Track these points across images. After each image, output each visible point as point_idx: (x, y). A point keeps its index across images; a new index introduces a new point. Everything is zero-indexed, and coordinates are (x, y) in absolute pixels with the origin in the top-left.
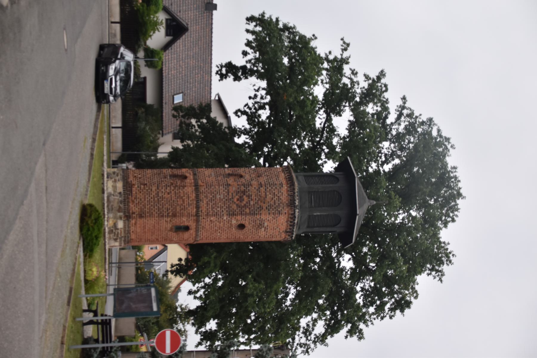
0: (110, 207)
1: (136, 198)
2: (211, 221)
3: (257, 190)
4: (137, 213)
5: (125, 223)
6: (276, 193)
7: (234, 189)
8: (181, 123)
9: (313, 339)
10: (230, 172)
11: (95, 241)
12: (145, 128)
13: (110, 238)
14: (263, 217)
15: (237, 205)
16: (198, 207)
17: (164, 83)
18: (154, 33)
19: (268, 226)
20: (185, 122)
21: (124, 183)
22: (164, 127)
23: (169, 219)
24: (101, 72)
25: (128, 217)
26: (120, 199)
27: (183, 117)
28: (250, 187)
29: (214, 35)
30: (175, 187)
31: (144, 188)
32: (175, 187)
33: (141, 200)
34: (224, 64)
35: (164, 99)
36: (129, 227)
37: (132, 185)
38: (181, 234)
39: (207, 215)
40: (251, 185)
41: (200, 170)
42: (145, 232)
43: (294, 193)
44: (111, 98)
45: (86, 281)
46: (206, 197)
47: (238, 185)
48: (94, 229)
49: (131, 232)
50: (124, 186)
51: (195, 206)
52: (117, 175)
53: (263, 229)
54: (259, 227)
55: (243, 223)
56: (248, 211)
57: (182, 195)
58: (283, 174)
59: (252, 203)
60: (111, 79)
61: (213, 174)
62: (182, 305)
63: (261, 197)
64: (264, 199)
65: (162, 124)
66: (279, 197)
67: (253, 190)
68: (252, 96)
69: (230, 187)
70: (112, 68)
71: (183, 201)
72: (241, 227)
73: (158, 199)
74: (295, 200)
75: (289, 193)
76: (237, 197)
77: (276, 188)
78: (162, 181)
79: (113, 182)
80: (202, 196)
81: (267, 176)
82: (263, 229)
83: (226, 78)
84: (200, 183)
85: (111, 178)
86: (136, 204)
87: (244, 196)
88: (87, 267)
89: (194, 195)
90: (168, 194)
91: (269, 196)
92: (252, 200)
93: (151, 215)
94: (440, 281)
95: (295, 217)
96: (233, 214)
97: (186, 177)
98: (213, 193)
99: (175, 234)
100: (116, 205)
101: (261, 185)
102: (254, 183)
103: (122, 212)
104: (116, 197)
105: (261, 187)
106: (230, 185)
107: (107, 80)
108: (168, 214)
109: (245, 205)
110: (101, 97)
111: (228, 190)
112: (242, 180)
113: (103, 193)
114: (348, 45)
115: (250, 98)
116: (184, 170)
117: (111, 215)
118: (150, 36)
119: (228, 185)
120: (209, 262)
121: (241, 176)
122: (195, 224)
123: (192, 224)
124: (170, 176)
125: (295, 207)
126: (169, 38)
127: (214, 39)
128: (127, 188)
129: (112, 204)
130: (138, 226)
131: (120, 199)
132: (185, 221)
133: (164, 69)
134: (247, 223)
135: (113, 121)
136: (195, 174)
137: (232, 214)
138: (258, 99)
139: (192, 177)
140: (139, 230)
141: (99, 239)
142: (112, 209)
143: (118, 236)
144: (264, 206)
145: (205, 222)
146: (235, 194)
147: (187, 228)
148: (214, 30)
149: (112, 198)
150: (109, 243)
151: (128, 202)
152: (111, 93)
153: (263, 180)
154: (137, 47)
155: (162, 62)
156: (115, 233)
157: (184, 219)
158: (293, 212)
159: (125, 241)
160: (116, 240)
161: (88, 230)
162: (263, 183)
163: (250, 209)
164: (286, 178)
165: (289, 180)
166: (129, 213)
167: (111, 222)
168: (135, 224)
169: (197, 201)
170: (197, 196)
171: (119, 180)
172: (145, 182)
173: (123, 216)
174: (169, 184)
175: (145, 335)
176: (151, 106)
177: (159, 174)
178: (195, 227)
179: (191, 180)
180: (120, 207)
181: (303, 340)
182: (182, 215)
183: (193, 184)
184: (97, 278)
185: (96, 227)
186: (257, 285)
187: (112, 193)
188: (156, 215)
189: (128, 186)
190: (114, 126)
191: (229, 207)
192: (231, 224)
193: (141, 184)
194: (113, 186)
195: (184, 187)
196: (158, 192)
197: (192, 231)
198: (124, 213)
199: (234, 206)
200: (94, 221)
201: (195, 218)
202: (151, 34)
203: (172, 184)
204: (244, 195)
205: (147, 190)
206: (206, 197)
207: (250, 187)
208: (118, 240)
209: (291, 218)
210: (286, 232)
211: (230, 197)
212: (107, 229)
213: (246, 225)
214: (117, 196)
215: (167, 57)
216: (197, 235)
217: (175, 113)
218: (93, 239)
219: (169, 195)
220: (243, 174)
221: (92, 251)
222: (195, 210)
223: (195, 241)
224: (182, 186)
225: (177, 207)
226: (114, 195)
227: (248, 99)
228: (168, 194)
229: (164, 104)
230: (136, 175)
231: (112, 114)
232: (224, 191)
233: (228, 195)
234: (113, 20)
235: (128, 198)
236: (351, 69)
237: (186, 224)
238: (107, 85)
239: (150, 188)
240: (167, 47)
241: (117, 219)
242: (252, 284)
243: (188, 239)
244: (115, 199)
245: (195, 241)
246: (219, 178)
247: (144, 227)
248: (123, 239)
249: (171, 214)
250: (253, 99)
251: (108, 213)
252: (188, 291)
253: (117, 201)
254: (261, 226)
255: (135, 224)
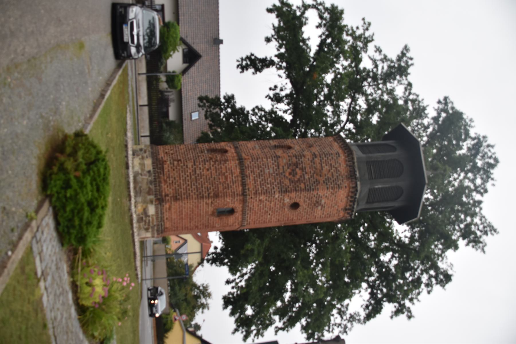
0: (138, 189)
1: (168, 177)
2: (260, 200)
3: (311, 161)
4: (172, 195)
5: (157, 208)
6: (333, 164)
7: (285, 161)
8: (206, 111)
9: (348, 318)
10: (277, 144)
11: (86, 214)
12: (169, 137)
13: (139, 228)
14: (321, 193)
15: (290, 180)
16: (244, 185)
17: (183, 102)
18: (174, 52)
19: (325, 203)
20: (210, 111)
21: (153, 160)
22: (185, 139)
23: (210, 201)
24: (118, 14)
25: (160, 200)
26: (150, 178)
27: (210, 107)
28: (303, 158)
29: (221, 65)
30: (215, 162)
31: (178, 165)
32: (215, 162)
33: (175, 178)
34: (244, 58)
35: (184, 115)
36: (162, 213)
37: (163, 163)
38: (224, 218)
39: (256, 193)
40: (304, 156)
41: (241, 143)
42: (182, 218)
43: (354, 163)
44: (133, 50)
45: (81, 310)
46: (253, 172)
47: (289, 156)
48: (82, 186)
49: (165, 218)
50: (153, 163)
51: (240, 183)
52: (145, 152)
53: (320, 208)
54: (315, 204)
55: (298, 201)
56: (302, 186)
57: (224, 171)
58: (336, 144)
59: (306, 177)
60: (132, 24)
61: (257, 146)
62: (203, 284)
63: (316, 169)
64: (320, 171)
65: (183, 136)
66: (336, 168)
67: (306, 161)
68: (273, 87)
69: (280, 159)
70: (132, 11)
71: (226, 178)
72: (295, 206)
73: (196, 177)
74: (355, 171)
75: (348, 163)
76: (289, 170)
77: (332, 158)
78: (198, 156)
79: (140, 159)
80: (248, 172)
81: (320, 146)
82: (320, 208)
83: (247, 70)
84: (244, 156)
85: (138, 155)
86: (170, 184)
87: (297, 170)
88: (79, 277)
89: (238, 170)
90: (208, 170)
91: (326, 168)
92: (306, 173)
93: (188, 197)
94: (482, 253)
95: (357, 190)
96: (286, 191)
97: (226, 151)
98: (261, 167)
99: (217, 219)
100: (145, 186)
101: (314, 155)
102: (306, 153)
103: (152, 194)
104: (144, 177)
105: (316, 157)
106: (279, 157)
107: (127, 24)
108: (209, 194)
109: (299, 180)
110: (120, 49)
111: (278, 163)
112: (292, 151)
113: (127, 168)
114: (369, 24)
115: (270, 89)
116: (223, 144)
117: (139, 199)
118: (171, 56)
119: (278, 157)
120: (252, 251)
121: (289, 148)
122: (241, 205)
123: (238, 206)
124: (208, 150)
125: (356, 178)
126: (186, 65)
127: (221, 69)
128: (157, 165)
129: (140, 185)
130: (174, 211)
131: (150, 178)
132: (229, 202)
133: (183, 90)
134: (302, 200)
135: (142, 131)
136: (236, 148)
137: (285, 191)
138: (278, 91)
139: (233, 150)
140: (174, 216)
141: (99, 211)
142: (141, 191)
143: (149, 225)
144: (321, 180)
145: (253, 203)
146: (286, 168)
147: (232, 212)
148: (221, 61)
149: (139, 178)
150: (138, 235)
151: (160, 182)
152: (133, 42)
153: (316, 150)
154: (159, 64)
155: (181, 85)
156: (145, 221)
157: (229, 200)
158: (354, 185)
159: (158, 230)
160: (147, 230)
161: (67, 185)
162: (317, 153)
163: (305, 183)
164: (340, 147)
165: (346, 149)
166: (161, 195)
167: (140, 208)
168: (170, 208)
169: (242, 177)
170: (242, 172)
171: (147, 157)
172: (179, 158)
173: (154, 199)
174: (208, 159)
175: (177, 310)
176: (173, 122)
177: (194, 149)
178: (241, 209)
179: (232, 153)
180: (150, 189)
181: (338, 320)
182: (225, 195)
183: (236, 158)
184: (106, 299)
185: (87, 180)
186: (306, 271)
187: (140, 171)
188: (194, 196)
189: (158, 164)
190: (142, 135)
191: (281, 183)
192: (284, 204)
193: (174, 160)
194: (140, 164)
195: (226, 161)
196: (195, 169)
197: (238, 215)
198: (156, 195)
199: (287, 182)
200: (84, 167)
201: (241, 198)
202: (172, 53)
203: (211, 159)
204: (297, 167)
205: (182, 167)
206: (253, 172)
207: (303, 158)
208: (150, 230)
209: (352, 192)
210: (345, 209)
211: (281, 171)
212: (134, 216)
213: (300, 204)
214: (145, 175)
215: (185, 81)
216: (243, 219)
217: (201, 104)
218: (81, 211)
219: (209, 172)
220: (292, 145)
221: (82, 239)
222: (241, 188)
223: (242, 226)
224: (223, 161)
225: (219, 186)
226: (141, 175)
227: (268, 90)
228: (208, 170)
229: (184, 120)
230: (167, 151)
231: (141, 125)
232: (273, 164)
233: (279, 168)
234: (140, 72)
235: (159, 177)
236: (375, 47)
237: (231, 206)
238: (126, 30)
239: (186, 164)
240: (184, 71)
241: (147, 203)
242: (301, 270)
243: (233, 224)
244: (143, 179)
245: (242, 226)
246: (266, 150)
247: (181, 212)
248: (156, 228)
249: (212, 194)
250: (273, 90)
251: (135, 196)
252: (226, 280)
253: (145, 181)
254: (317, 203)
255: (170, 208)
